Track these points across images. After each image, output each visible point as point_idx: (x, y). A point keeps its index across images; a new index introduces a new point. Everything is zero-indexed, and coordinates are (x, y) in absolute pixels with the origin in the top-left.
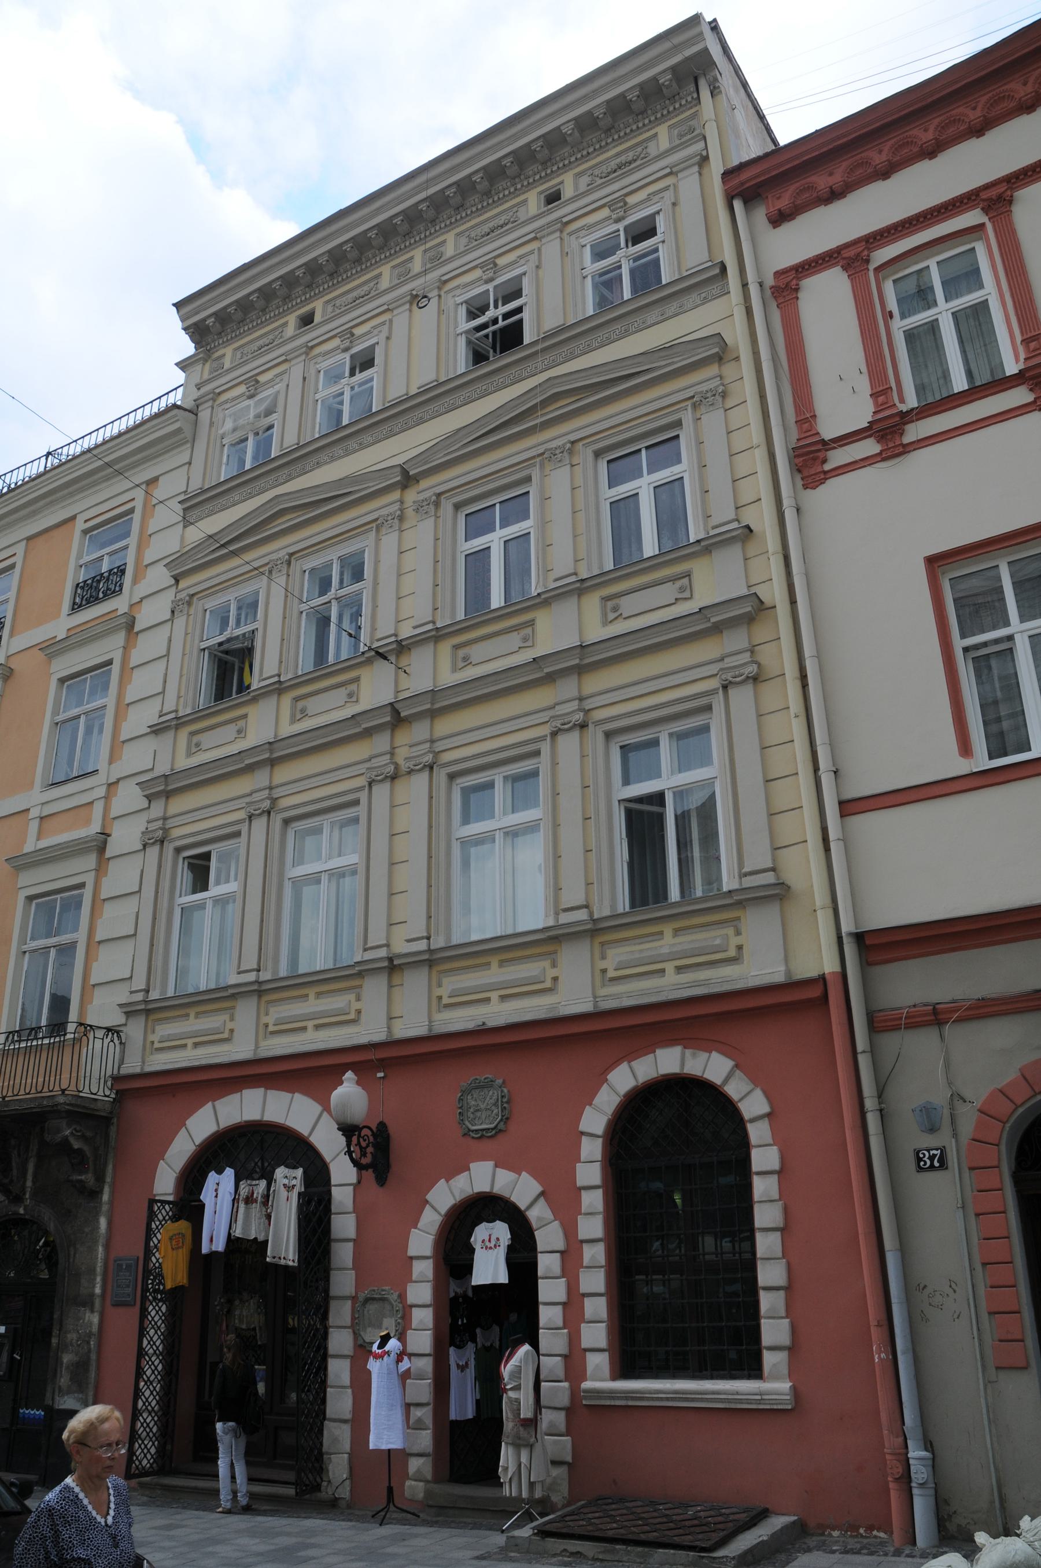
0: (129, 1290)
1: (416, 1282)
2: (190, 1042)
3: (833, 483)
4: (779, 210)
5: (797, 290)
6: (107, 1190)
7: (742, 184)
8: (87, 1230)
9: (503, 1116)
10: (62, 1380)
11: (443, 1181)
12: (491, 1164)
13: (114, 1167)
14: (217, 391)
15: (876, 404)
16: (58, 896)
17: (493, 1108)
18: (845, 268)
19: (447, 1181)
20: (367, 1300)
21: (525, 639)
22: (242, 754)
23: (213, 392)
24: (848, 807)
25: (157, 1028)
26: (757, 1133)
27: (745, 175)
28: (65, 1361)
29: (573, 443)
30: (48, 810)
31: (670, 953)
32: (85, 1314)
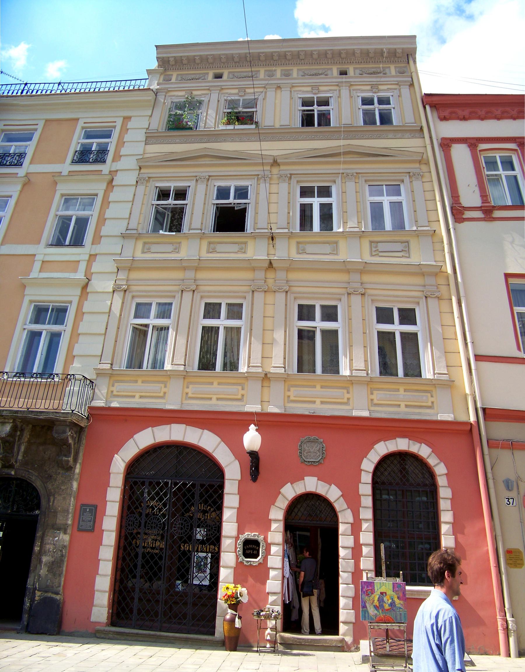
0: (92, 523)
2: (138, 395)
5: (450, 147)
6: (78, 466)
8: (63, 488)
10: (42, 571)
11: (289, 484)
12: (316, 478)
13: (84, 455)
16: (51, 304)
17: (317, 452)
19: (291, 484)
25: (116, 384)
28: (44, 560)
30: (47, 258)
32: (59, 535)
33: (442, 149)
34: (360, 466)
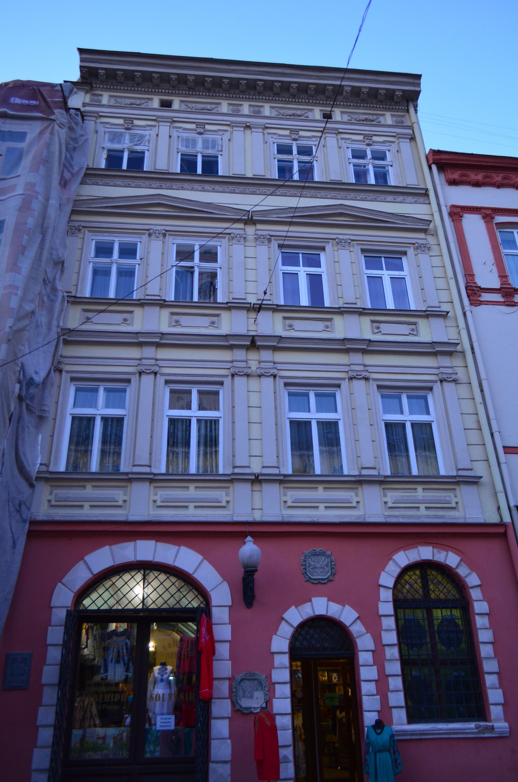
1: (277, 668)
3: (483, 306)
4: (454, 179)
5: (462, 217)
7: (441, 159)
9: (332, 572)
11: (294, 607)
12: (326, 599)
14: (101, 114)
15: (501, 281)
17: (325, 567)
18: (484, 218)
19: (296, 607)
20: (242, 680)
21: (327, 327)
22: (139, 335)
23: (97, 113)
24: (508, 450)
26: (475, 594)
27: (443, 156)
29: (271, 236)
31: (423, 500)
33: (451, 219)
34: (378, 582)
